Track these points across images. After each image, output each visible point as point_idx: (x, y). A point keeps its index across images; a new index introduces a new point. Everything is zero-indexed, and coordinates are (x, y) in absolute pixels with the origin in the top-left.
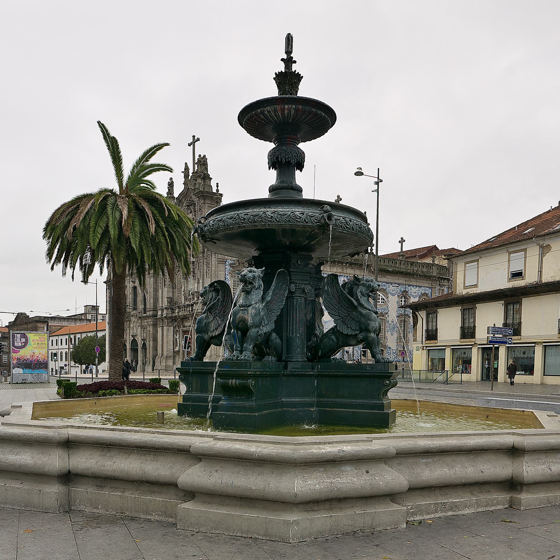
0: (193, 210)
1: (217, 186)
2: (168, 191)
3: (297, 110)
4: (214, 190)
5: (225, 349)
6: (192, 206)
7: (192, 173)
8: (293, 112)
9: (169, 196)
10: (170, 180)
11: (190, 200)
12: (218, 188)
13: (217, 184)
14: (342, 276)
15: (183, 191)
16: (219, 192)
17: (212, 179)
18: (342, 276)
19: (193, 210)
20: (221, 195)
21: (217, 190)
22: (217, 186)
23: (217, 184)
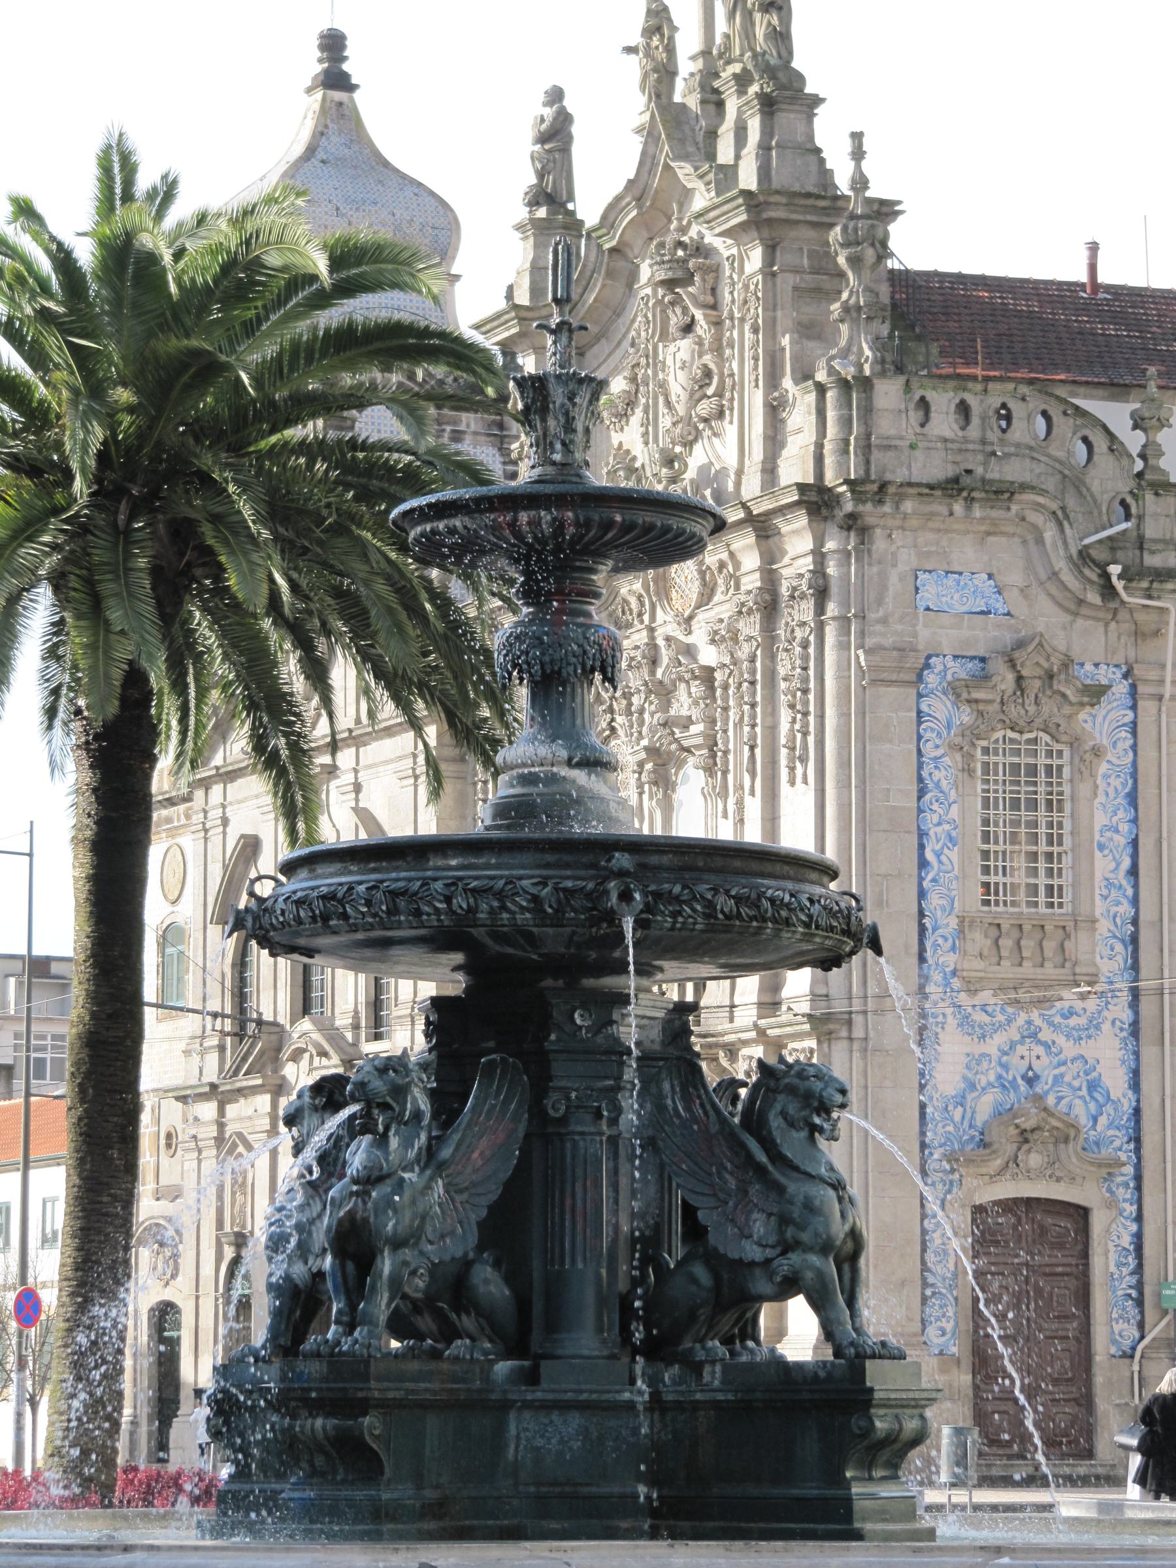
0: (699, 315)
1: (858, 154)
2: (533, 180)
3: (559, 526)
4: (843, 182)
5: (928, 1292)
6: (692, 283)
7: (693, 58)
8: (547, 529)
9: (542, 213)
10: (545, 104)
11: (680, 244)
12: (864, 164)
13: (857, 137)
15: (630, 181)
16: (868, 194)
17: (823, 100)
19: (699, 315)
20: (885, 211)
21: (860, 182)
22: (858, 154)
23: (857, 137)
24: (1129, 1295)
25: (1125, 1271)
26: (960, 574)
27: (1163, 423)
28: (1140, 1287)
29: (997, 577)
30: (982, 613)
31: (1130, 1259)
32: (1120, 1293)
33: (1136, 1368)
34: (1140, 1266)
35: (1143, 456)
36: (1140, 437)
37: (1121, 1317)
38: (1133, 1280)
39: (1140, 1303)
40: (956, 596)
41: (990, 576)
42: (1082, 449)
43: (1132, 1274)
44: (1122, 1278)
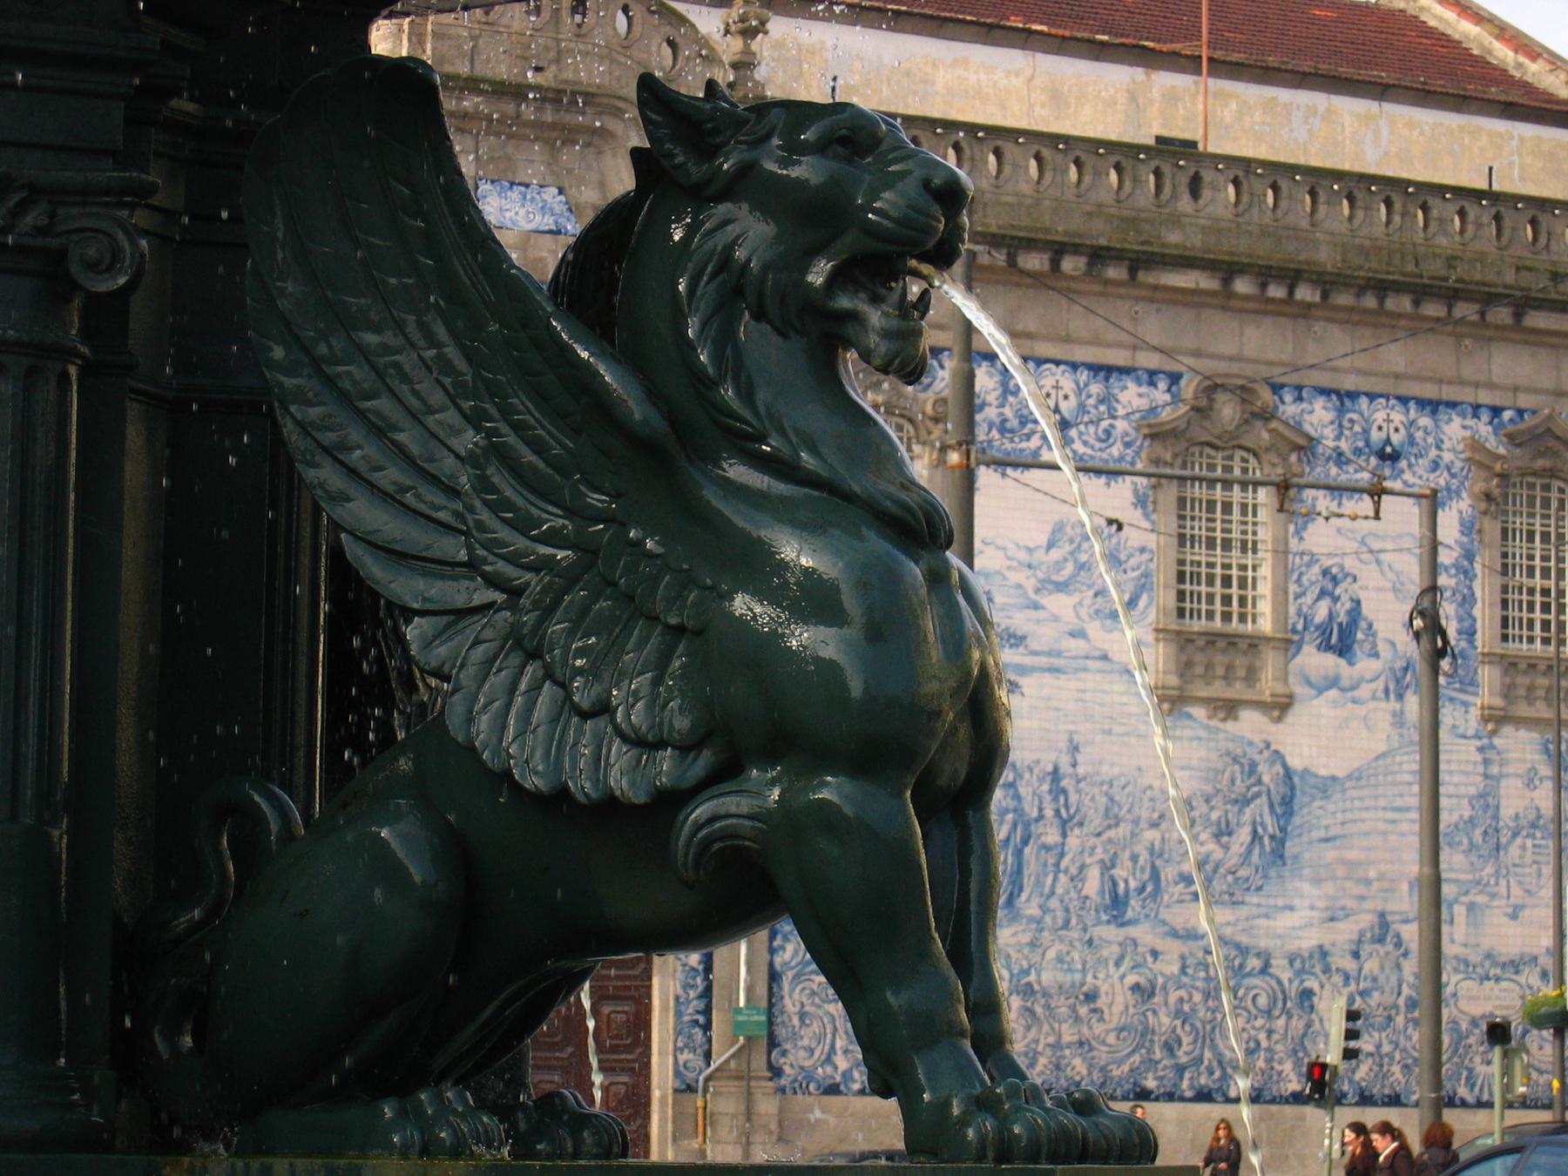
14: (1452, 405)
18: (1452, 405)
24: (696, 1022)
25: (692, 994)
26: (527, 186)
27: (761, 28)
28: (707, 1012)
29: (568, 191)
30: (551, 232)
31: (699, 980)
32: (686, 1018)
33: (700, 1103)
34: (707, 993)
35: (735, 66)
36: (736, 44)
37: (686, 1046)
38: (701, 1005)
39: (707, 1027)
40: (522, 212)
41: (561, 191)
42: (667, 51)
43: (700, 997)
44: (689, 1002)
